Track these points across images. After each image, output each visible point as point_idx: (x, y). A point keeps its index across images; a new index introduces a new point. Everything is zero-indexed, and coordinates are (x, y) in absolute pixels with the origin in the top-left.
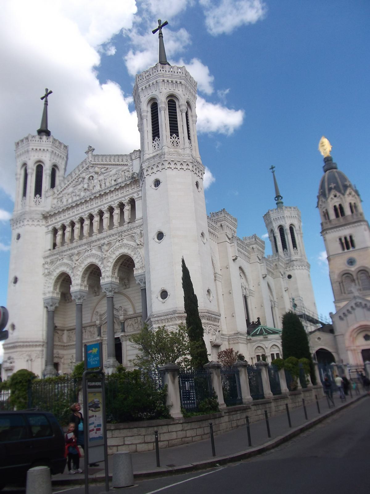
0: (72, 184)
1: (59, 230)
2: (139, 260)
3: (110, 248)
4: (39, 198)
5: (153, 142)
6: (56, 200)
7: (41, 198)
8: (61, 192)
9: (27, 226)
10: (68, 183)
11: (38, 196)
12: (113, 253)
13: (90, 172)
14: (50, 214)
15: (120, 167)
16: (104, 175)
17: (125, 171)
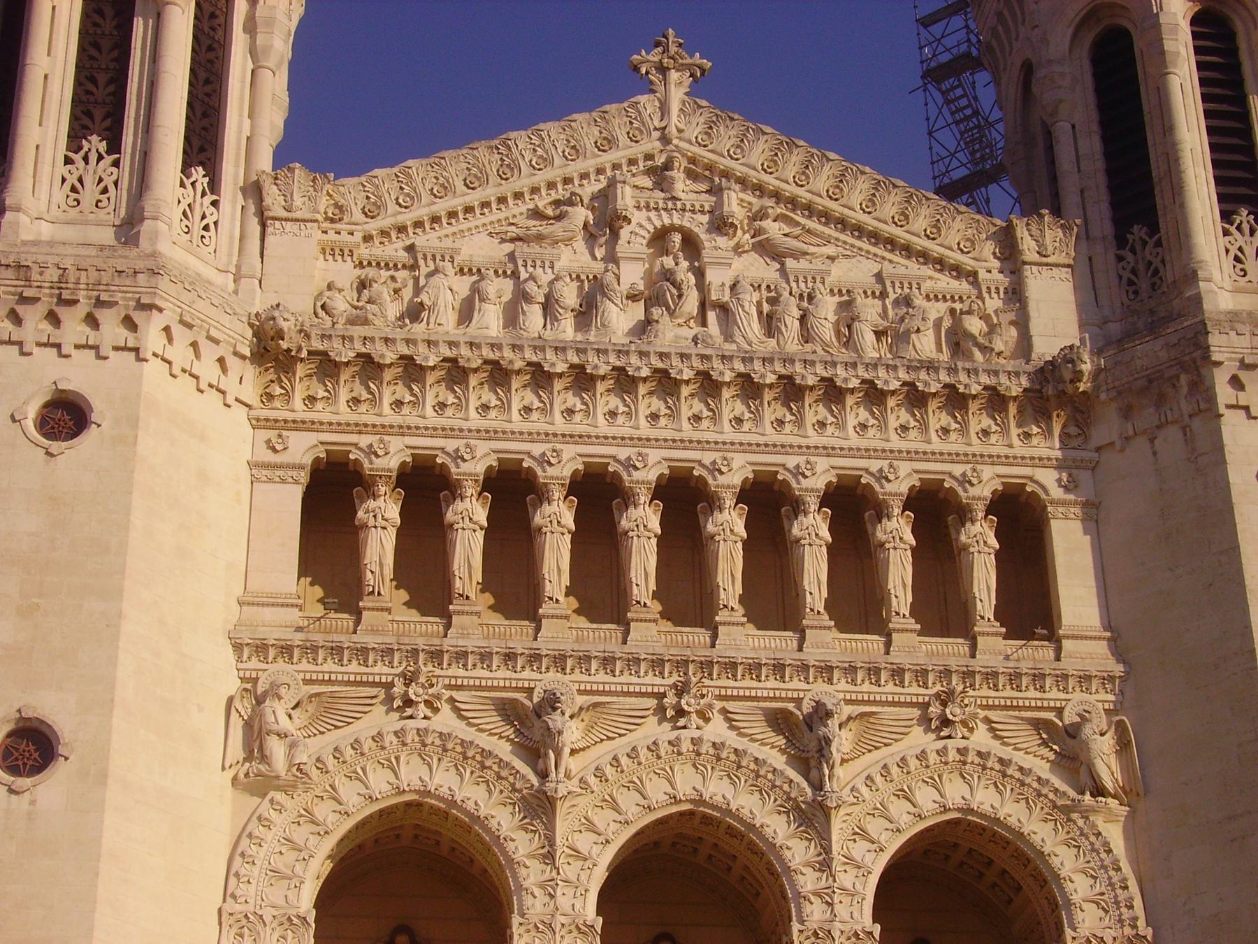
0: (495, 215)
1: (383, 489)
2: (1098, 889)
3: (865, 746)
4: (203, 194)
5: (1226, 233)
6: (345, 273)
7: (215, 204)
8: (402, 229)
9: (154, 368)
10: (474, 198)
11: (198, 173)
12: (892, 788)
13: (674, 198)
14: (317, 345)
15: (913, 268)
16: (790, 263)
17: (958, 306)
